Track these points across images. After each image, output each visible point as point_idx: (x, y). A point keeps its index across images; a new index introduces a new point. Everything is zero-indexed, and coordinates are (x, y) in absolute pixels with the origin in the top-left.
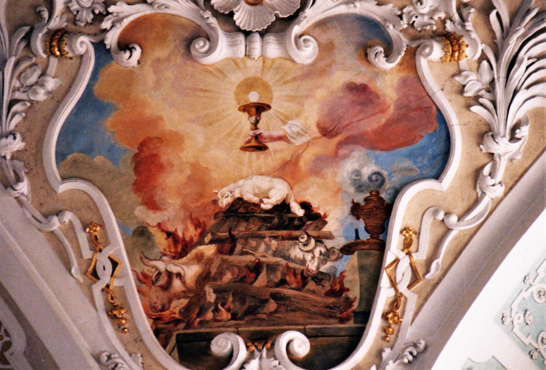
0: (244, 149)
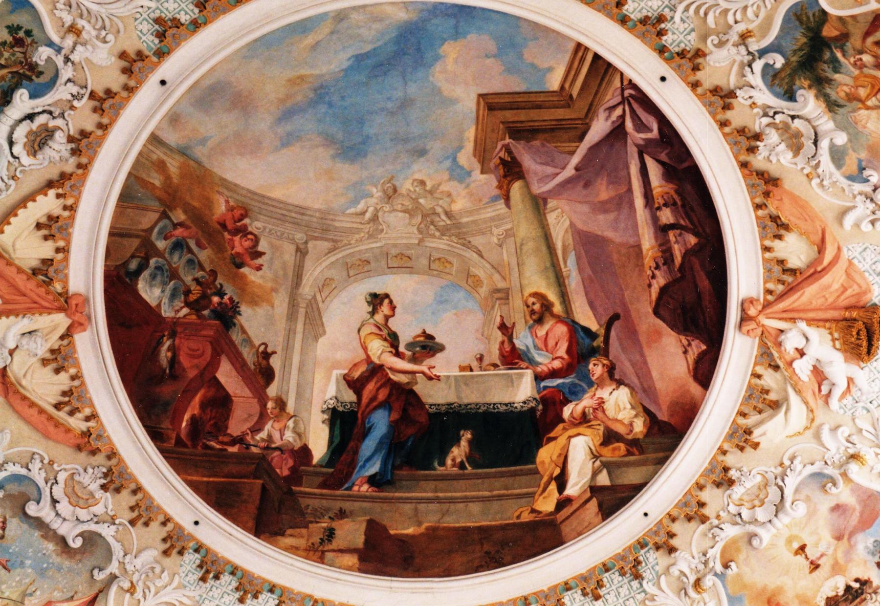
0: (811, 572)
